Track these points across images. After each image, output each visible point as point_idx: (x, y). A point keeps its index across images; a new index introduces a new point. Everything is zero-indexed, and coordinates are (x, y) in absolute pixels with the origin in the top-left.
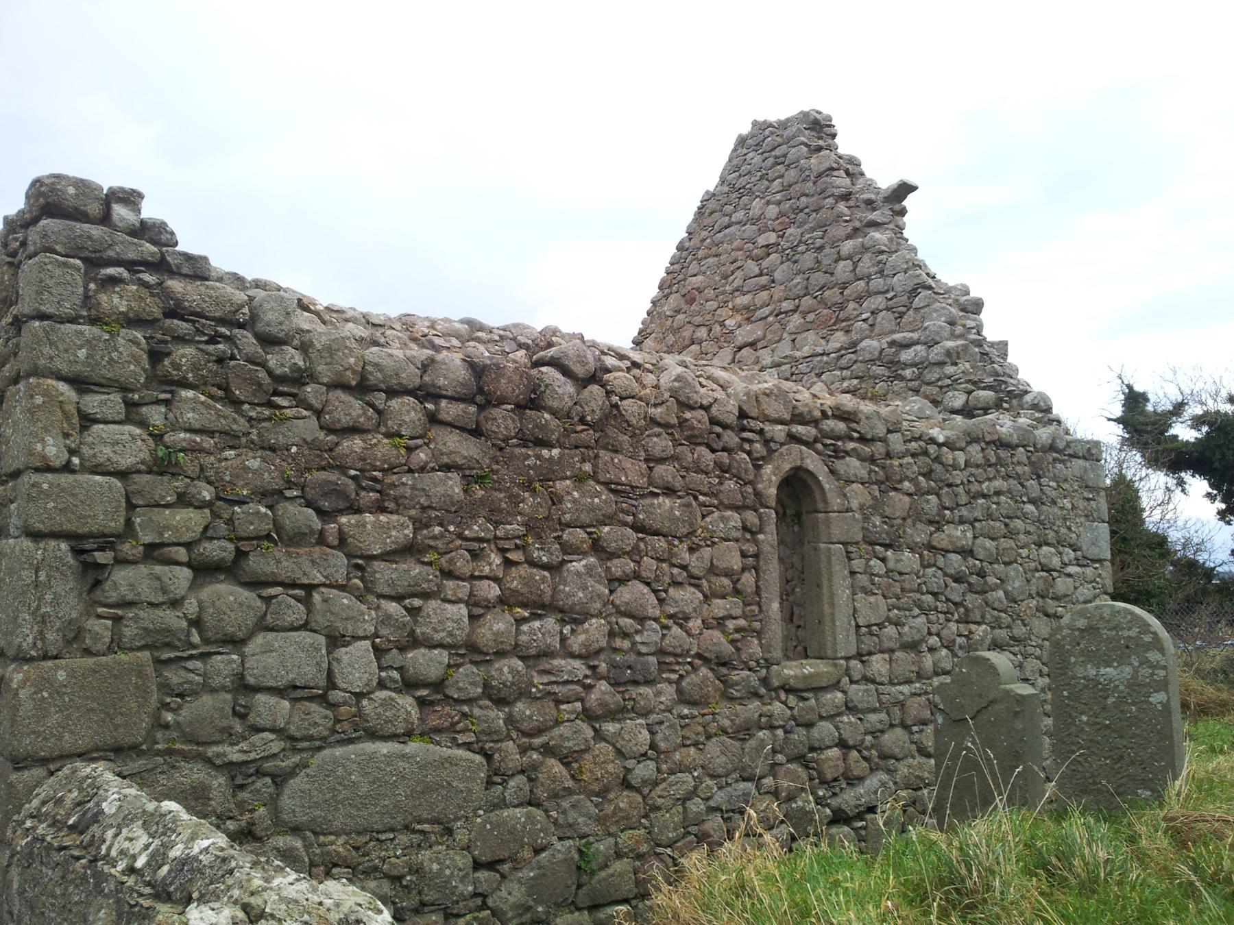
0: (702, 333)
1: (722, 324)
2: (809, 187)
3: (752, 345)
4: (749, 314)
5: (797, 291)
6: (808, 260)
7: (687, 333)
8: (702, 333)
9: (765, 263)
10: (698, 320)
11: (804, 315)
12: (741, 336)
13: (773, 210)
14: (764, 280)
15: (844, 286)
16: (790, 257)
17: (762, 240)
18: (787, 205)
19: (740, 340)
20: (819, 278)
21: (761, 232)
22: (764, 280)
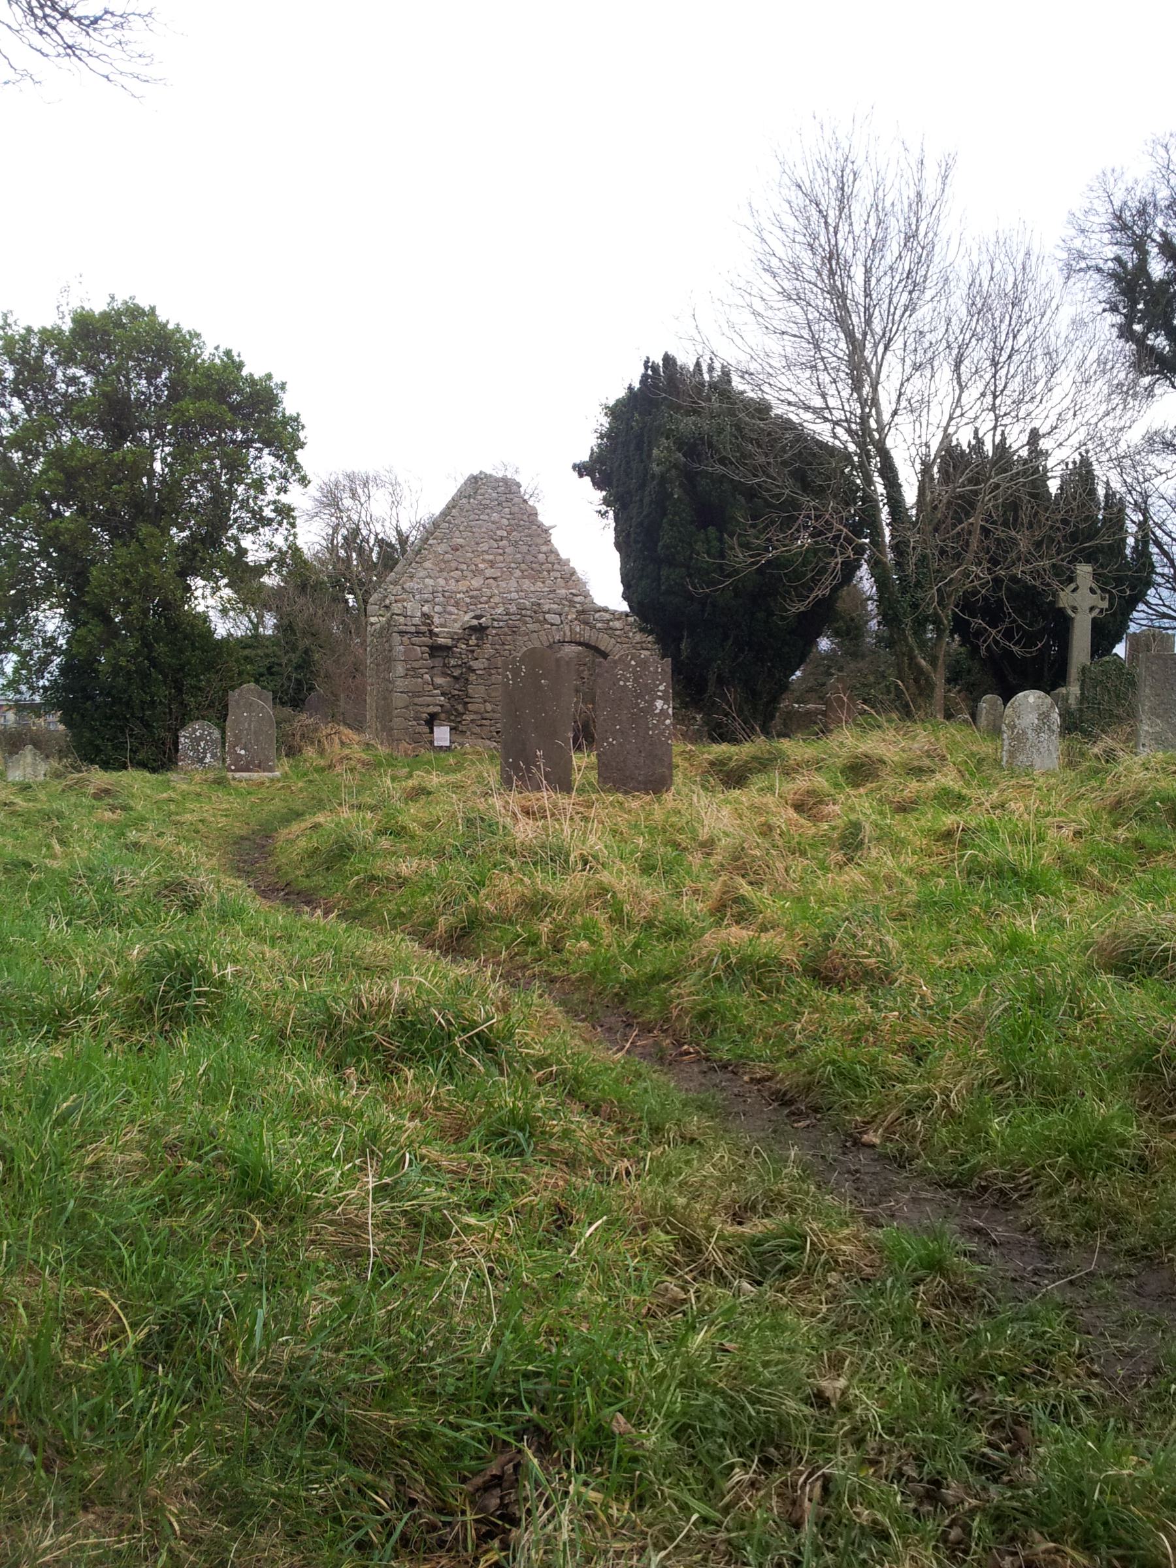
0: (464, 567)
1: (476, 565)
2: (525, 518)
3: (494, 578)
4: (492, 564)
5: (520, 560)
6: (525, 549)
7: (454, 565)
8: (464, 567)
9: (501, 543)
10: (461, 560)
11: (522, 572)
12: (489, 572)
13: (505, 522)
14: (501, 551)
15: (542, 564)
16: (515, 545)
17: (499, 533)
18: (513, 522)
19: (488, 575)
20: (529, 558)
21: (498, 529)
22: (501, 551)
